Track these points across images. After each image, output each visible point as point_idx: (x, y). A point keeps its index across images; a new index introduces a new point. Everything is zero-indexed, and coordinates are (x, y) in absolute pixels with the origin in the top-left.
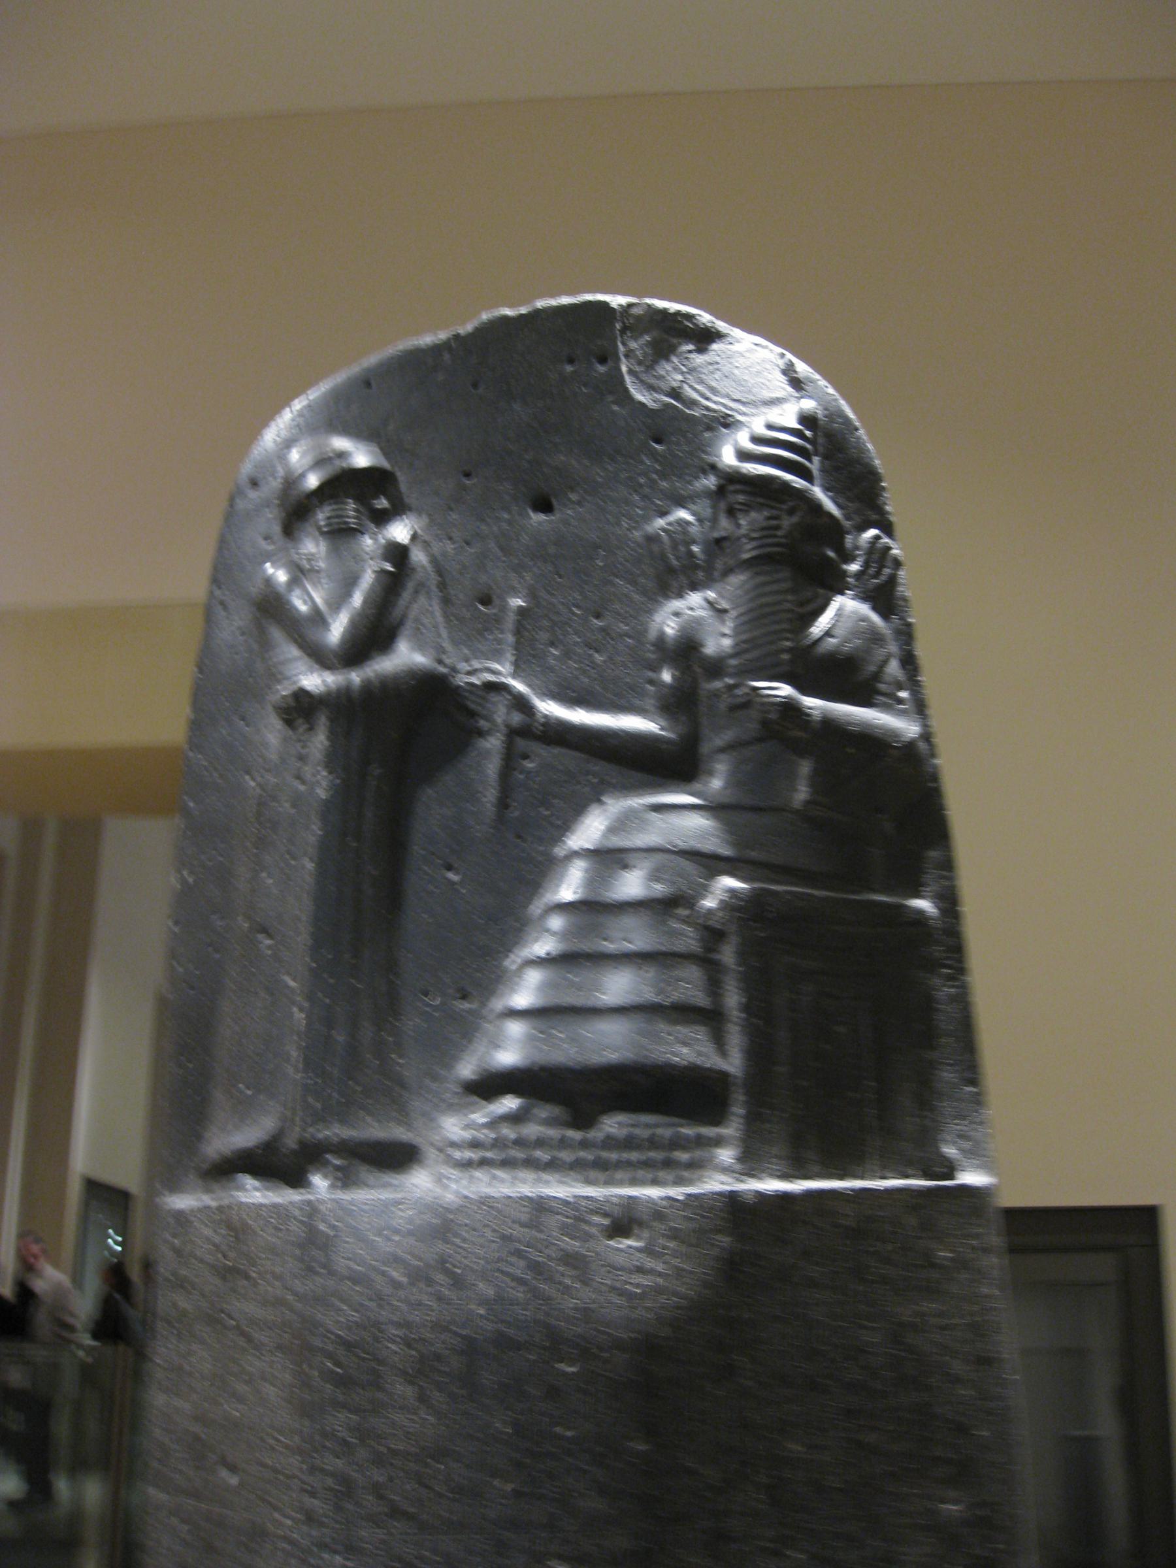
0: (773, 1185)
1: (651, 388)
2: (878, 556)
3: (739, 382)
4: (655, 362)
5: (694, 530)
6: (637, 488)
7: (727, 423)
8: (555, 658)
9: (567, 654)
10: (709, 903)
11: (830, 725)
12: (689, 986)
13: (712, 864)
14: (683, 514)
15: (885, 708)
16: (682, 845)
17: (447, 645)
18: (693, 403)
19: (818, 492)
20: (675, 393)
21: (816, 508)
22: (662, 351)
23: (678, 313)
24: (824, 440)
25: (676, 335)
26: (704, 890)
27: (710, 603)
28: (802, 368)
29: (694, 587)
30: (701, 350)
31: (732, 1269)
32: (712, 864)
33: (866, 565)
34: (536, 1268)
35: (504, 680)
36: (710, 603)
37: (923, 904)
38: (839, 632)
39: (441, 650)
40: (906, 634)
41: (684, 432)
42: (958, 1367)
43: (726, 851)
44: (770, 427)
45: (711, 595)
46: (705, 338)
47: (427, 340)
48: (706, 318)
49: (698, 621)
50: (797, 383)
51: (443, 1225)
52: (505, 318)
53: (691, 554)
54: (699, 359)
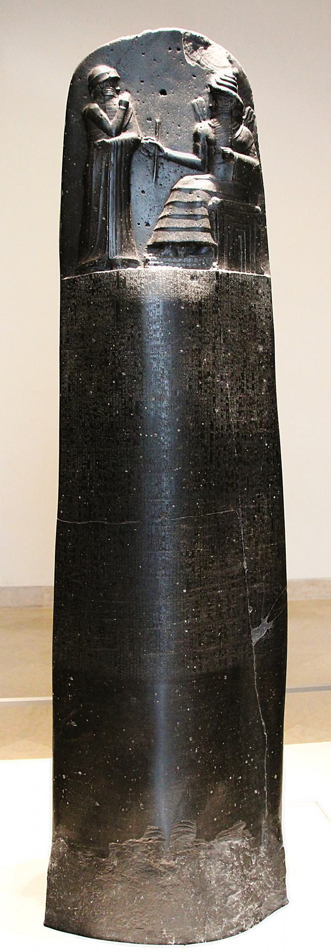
2: (251, 115)
6: (188, 90)
7: (212, 72)
9: (171, 136)
10: (210, 203)
11: (240, 160)
12: (206, 223)
13: (211, 194)
14: (200, 99)
15: (252, 156)
18: (203, 66)
20: (198, 62)
22: (195, 48)
24: (240, 80)
25: (198, 43)
28: (233, 58)
30: (205, 49)
31: (217, 288)
34: (176, 286)
37: (257, 207)
40: (256, 137)
41: (200, 73)
43: (215, 191)
46: (206, 45)
47: (128, 38)
48: (206, 39)
50: (231, 62)
54: (204, 52)
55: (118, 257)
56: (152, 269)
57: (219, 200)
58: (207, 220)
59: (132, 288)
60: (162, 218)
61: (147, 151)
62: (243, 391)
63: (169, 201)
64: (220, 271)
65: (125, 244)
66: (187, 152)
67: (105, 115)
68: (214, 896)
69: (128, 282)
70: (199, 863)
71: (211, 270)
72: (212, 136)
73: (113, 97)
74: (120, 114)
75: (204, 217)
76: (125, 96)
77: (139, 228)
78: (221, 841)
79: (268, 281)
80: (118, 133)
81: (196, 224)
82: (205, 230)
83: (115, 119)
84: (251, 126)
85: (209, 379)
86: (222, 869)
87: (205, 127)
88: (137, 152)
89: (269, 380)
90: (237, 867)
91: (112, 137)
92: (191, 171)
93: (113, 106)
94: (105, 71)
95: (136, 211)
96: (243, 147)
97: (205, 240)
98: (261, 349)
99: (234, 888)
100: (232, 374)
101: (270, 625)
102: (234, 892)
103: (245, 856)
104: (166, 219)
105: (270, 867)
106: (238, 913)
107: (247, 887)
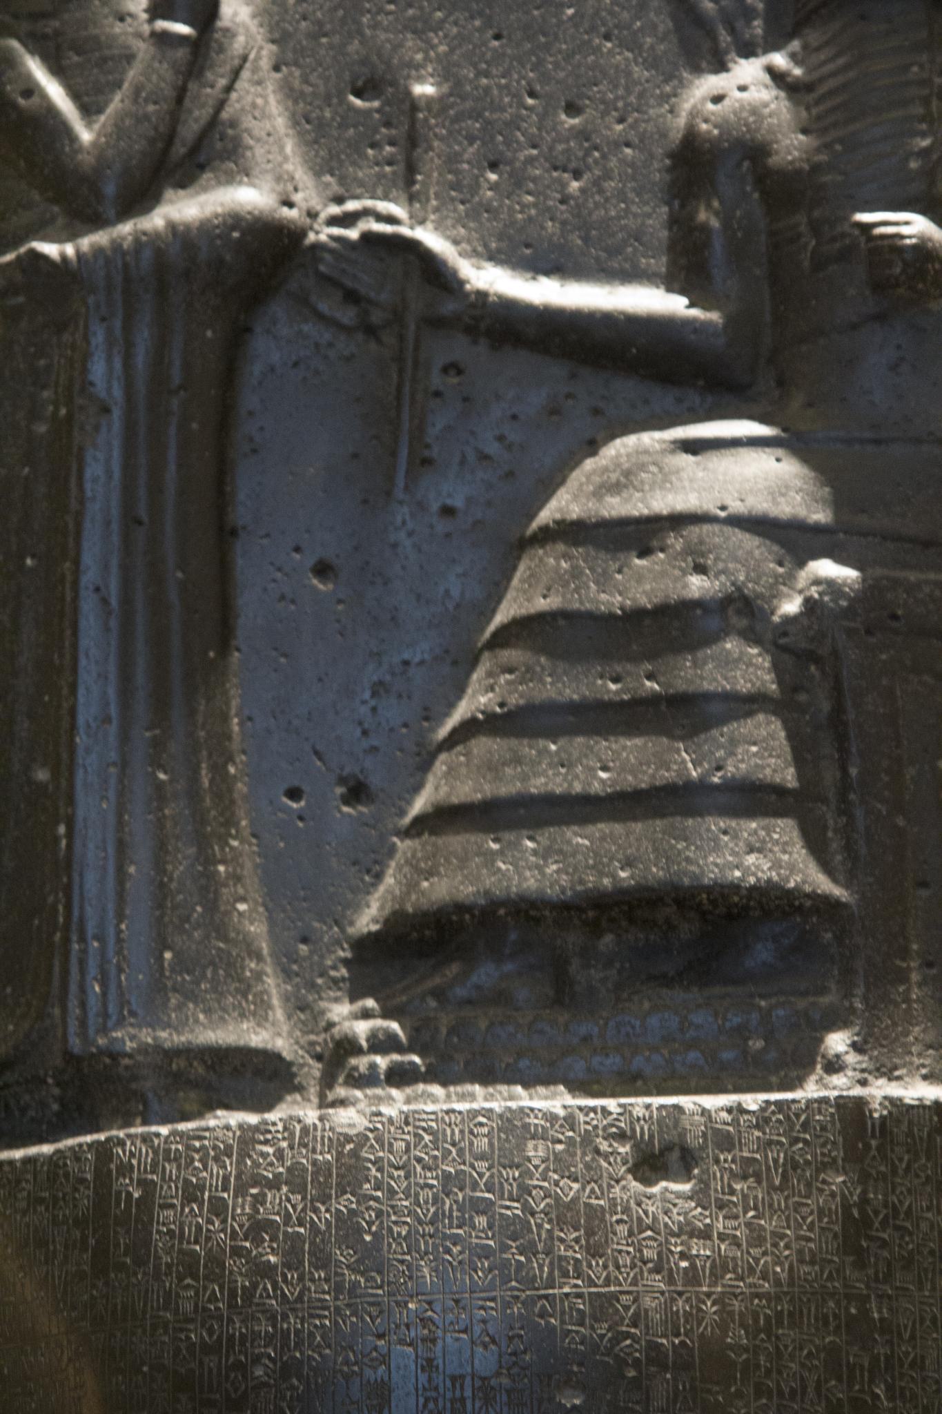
8: (494, 187)
9: (517, 181)
10: (791, 606)
12: (759, 750)
13: (793, 540)
16: (736, 507)
27: (777, 76)
29: (748, 50)
34: (514, 1230)
35: (405, 231)
36: (777, 76)
43: (820, 516)
45: (779, 60)
51: (349, 1165)
57: (846, 574)
59: (189, 1264)
61: (352, 297)
63: (499, 619)
64: (880, 1090)
66: (630, 275)
71: (811, 1090)
72: (792, 146)
74: (144, 69)
81: (686, 763)
83: (116, 103)
88: (278, 309)
91: (97, 221)
97: (755, 868)
104: (482, 745)
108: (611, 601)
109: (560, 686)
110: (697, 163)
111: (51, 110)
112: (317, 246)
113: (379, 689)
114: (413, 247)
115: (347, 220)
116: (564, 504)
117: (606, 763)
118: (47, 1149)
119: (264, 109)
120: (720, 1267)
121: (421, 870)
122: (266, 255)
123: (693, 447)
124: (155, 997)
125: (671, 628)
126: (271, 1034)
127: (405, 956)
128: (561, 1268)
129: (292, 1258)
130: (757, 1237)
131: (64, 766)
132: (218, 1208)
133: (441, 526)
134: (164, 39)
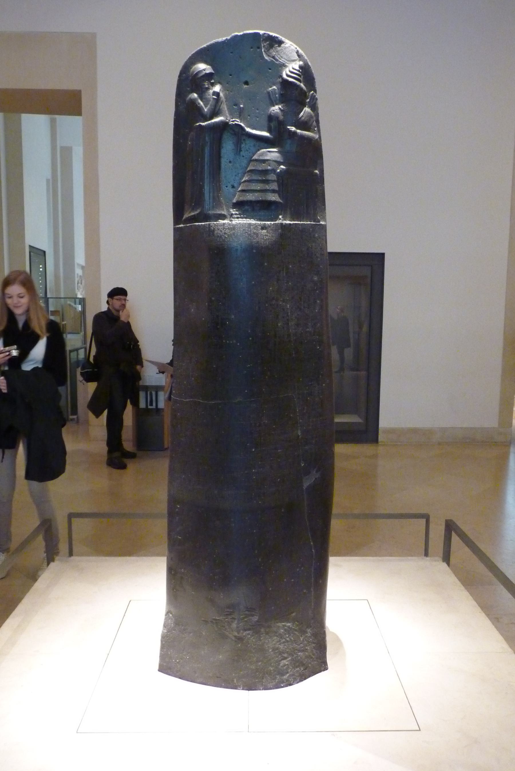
0: (288, 222)
1: (269, 56)
3: (287, 55)
4: (269, 49)
5: (277, 91)
10: (278, 171)
12: (274, 186)
13: (279, 163)
14: (275, 87)
15: (312, 132)
16: (273, 159)
17: (228, 115)
18: (277, 60)
19: (302, 85)
20: (274, 57)
21: (302, 89)
22: (271, 46)
23: (274, 36)
26: (277, 168)
27: (280, 109)
28: (301, 51)
29: (277, 104)
30: (279, 46)
31: (281, 236)
32: (279, 163)
33: (310, 100)
34: (249, 235)
36: (280, 109)
37: (317, 171)
38: (304, 116)
39: (226, 116)
40: (317, 115)
42: (318, 255)
43: (282, 161)
44: (293, 69)
47: (220, 40)
49: (277, 112)
51: (234, 228)
52: (237, 35)
53: (276, 97)
54: (279, 49)
55: (211, 212)
56: (235, 222)
57: (284, 167)
58: (276, 184)
59: (218, 236)
60: (243, 182)
61: (234, 131)
62: (300, 309)
63: (248, 169)
64: (284, 222)
65: (217, 203)
67: (201, 103)
68: (270, 660)
69: (216, 232)
70: (260, 637)
72: (281, 118)
73: (208, 89)
75: (273, 181)
76: (217, 88)
77: (226, 190)
78: (277, 622)
79: (324, 227)
80: (211, 118)
81: (267, 187)
82: (274, 191)
83: (209, 106)
84: (314, 107)
85: (274, 302)
86: (278, 642)
87: (276, 109)
89: (322, 301)
90: (288, 641)
92: (266, 145)
93: (209, 97)
94: (202, 67)
95: (225, 177)
96: (305, 125)
98: (316, 278)
99: (286, 655)
100: (293, 298)
101: (318, 475)
102: (285, 658)
103: (295, 634)
104: (246, 183)
105: (314, 643)
106: (288, 673)
107: (295, 656)
108: (260, 169)
109: (255, 177)
110: (271, 118)
111: (202, 107)
112: (230, 125)
113: (236, 175)
114: (240, 125)
115: (233, 121)
116: (255, 157)
117: (259, 186)
118: (203, 223)
119: (224, 107)
120: (269, 239)
121: (240, 196)
122: (224, 125)
123: (269, 152)
124: (213, 208)
125: (265, 172)
126: (224, 212)
127: (239, 205)
128: (254, 239)
129: (228, 235)
130: (272, 236)
131: (204, 183)
132: (221, 231)
133: (242, 158)
134: (214, 98)
